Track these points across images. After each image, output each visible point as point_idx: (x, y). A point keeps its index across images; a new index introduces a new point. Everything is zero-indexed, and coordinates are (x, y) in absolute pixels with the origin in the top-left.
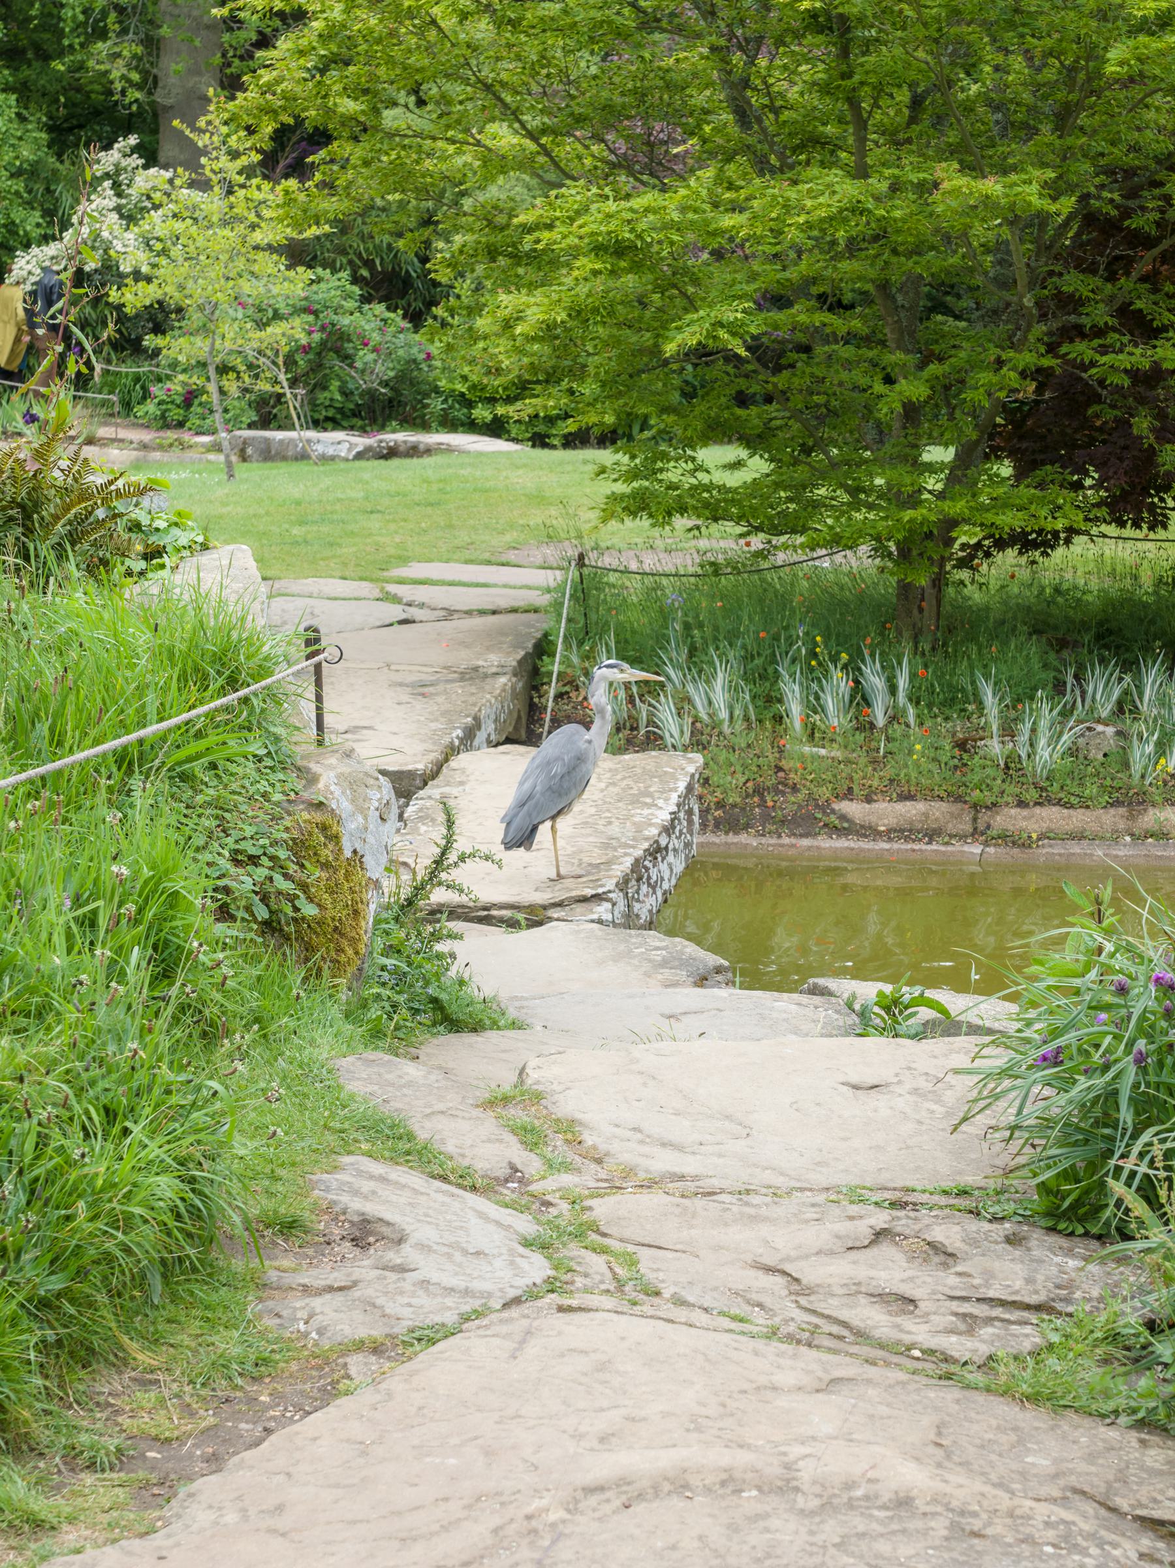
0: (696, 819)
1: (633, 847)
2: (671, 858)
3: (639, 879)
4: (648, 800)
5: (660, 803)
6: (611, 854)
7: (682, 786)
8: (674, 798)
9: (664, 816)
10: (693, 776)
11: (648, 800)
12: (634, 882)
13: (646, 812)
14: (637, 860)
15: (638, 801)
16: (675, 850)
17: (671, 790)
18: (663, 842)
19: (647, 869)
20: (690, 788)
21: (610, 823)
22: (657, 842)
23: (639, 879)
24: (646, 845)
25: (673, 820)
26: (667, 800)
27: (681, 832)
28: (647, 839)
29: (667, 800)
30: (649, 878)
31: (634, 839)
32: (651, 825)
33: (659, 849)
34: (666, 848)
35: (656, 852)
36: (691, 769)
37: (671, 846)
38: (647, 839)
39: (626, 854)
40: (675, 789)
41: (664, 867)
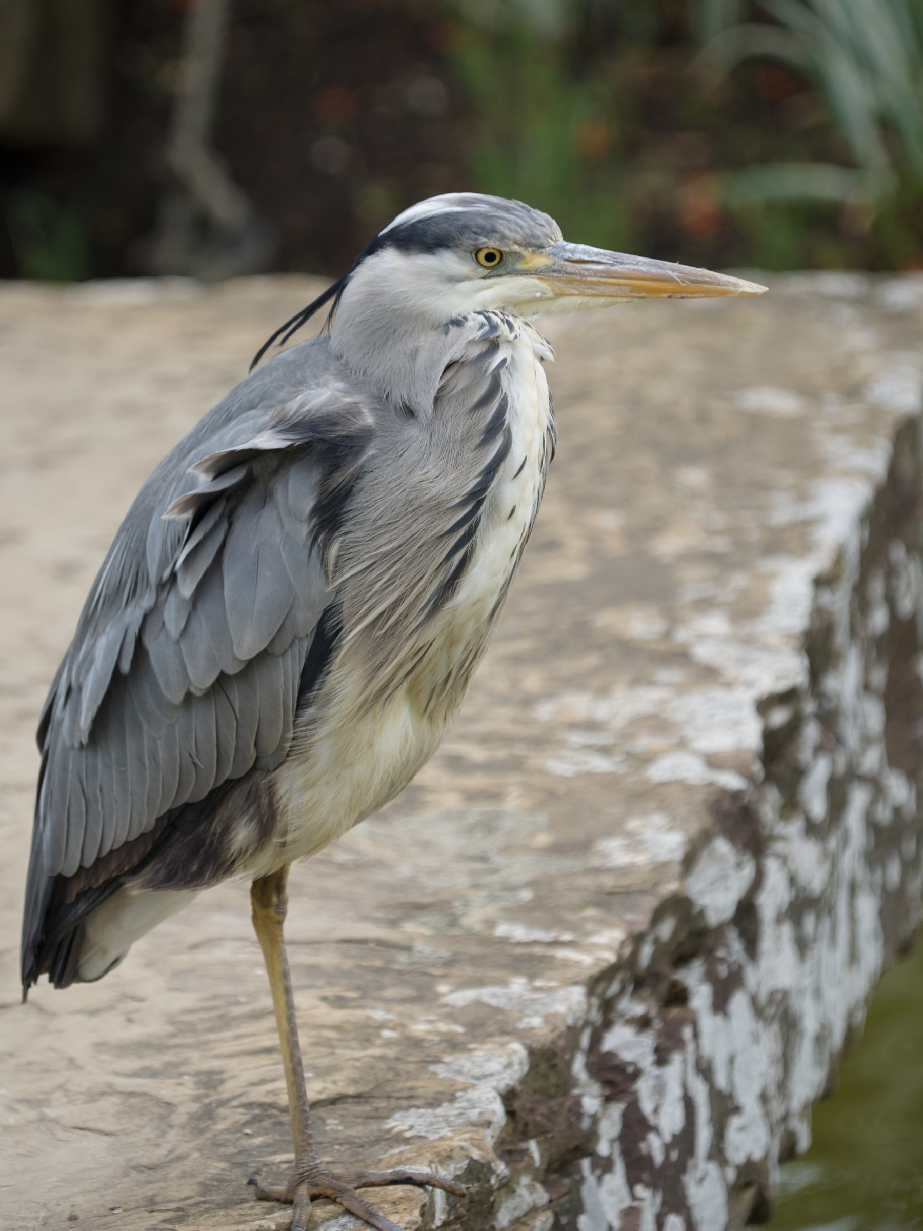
1: (529, 962)
4: (640, 624)
7: (839, 509)
11: (640, 624)
13: (623, 705)
15: (582, 637)
24: (605, 943)
25: (777, 749)
29: (746, 610)
32: (647, 796)
38: (609, 900)
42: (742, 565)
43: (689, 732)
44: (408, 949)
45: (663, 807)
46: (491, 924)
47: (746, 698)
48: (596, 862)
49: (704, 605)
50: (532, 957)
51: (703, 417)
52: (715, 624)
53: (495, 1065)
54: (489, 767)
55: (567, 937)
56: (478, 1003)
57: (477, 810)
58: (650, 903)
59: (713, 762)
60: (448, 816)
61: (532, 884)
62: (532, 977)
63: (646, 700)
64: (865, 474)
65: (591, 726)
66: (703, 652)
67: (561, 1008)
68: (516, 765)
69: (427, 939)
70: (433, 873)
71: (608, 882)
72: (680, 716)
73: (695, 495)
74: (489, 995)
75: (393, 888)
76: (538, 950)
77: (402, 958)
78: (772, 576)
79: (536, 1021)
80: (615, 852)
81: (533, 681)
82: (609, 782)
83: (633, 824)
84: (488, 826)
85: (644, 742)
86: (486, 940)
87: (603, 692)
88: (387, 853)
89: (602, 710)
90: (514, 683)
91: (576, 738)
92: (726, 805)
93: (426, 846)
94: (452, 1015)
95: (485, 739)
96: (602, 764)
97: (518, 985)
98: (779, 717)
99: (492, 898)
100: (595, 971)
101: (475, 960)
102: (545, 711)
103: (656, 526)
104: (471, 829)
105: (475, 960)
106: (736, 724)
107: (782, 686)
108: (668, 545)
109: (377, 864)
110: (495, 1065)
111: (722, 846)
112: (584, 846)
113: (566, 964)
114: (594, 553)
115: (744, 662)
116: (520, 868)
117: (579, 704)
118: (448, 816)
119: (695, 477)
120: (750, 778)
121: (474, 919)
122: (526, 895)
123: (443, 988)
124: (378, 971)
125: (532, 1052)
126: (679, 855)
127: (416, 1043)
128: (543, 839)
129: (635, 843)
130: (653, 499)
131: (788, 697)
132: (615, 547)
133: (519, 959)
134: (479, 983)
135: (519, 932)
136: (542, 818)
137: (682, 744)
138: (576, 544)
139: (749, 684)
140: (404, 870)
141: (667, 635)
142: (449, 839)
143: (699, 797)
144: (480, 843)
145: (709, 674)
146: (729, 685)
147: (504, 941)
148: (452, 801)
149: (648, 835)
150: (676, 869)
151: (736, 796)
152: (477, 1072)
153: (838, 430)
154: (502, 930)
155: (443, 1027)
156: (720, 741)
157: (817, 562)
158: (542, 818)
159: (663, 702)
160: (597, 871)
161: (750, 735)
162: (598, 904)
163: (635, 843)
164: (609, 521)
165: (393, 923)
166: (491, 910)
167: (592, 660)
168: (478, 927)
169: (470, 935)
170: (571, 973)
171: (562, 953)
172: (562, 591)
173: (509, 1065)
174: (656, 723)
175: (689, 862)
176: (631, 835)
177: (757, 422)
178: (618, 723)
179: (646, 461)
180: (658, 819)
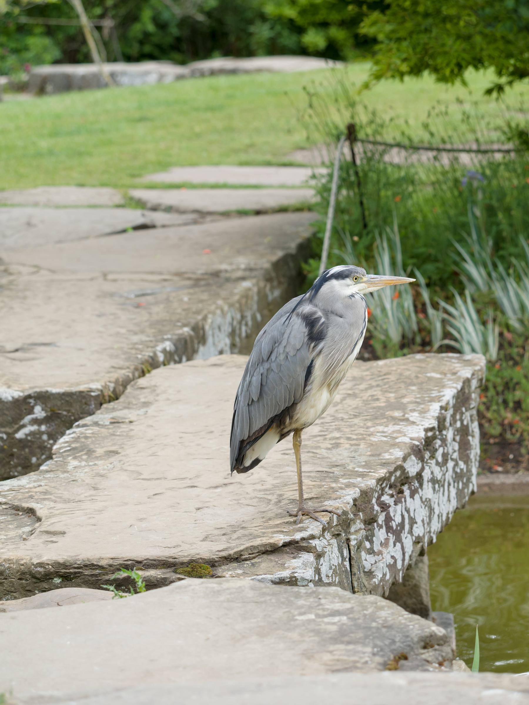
0: (475, 441)
1: (363, 475)
2: (427, 491)
3: (370, 521)
4: (397, 414)
5: (414, 416)
6: (327, 484)
7: (449, 394)
8: (435, 409)
9: (416, 433)
10: (467, 382)
11: (397, 414)
12: (358, 525)
13: (391, 428)
14: (365, 494)
15: (383, 416)
16: (434, 481)
17: (432, 400)
18: (412, 467)
19: (384, 507)
20: (462, 398)
21: (337, 445)
22: (401, 468)
23: (370, 521)
24: (382, 472)
26: (423, 412)
27: (445, 456)
28: (384, 464)
29: (423, 412)
30: (388, 519)
31: (367, 465)
32: (395, 445)
33: (405, 479)
34: (419, 476)
35: (401, 483)
36: (466, 373)
37: (426, 475)
38: (384, 464)
39: (348, 486)
40: (439, 399)
41: (414, 504)
42: (423, 404)
43: (406, 433)
44: (333, 473)
45: (398, 447)
46: (354, 468)
47: (422, 428)
48: (382, 458)
49: (413, 410)
50: (363, 474)
51: (417, 377)
52: (416, 414)
53: (351, 492)
54: (357, 439)
55: (372, 471)
56: (349, 482)
57: (353, 448)
58: (394, 466)
59: (412, 439)
60: (346, 449)
61: (365, 462)
62: (363, 478)
63: (397, 428)
64: (456, 388)
65: (383, 432)
66: (411, 419)
67: (370, 483)
68: (364, 439)
69: (338, 471)
70: (341, 460)
71: (384, 461)
72: (404, 431)
73: (413, 391)
74: (351, 480)
75: (331, 462)
76: (365, 473)
77: (332, 474)
78: (431, 405)
79: (363, 485)
80: (387, 456)
81: (369, 424)
82: (386, 442)
83: (391, 451)
84: (355, 451)
85: (395, 435)
86: (352, 471)
87: (387, 426)
88: (330, 456)
89: (386, 429)
90: (365, 424)
91: (379, 434)
92: (415, 448)
93: (340, 455)
94: (342, 484)
95: (356, 435)
96: (385, 439)
97: (359, 479)
98: (430, 434)
99: (355, 464)
100: (379, 477)
101: (349, 475)
102: (372, 429)
103: (403, 397)
104: (352, 452)
105: (349, 475)
106: (418, 432)
107: (431, 426)
108: (405, 400)
109: (327, 458)
110: (351, 492)
111: (413, 457)
112: (379, 455)
113: (372, 476)
114: (388, 401)
115: (422, 421)
116: (363, 459)
117: (381, 428)
118: (346, 449)
119: (414, 388)
120: (421, 443)
121: (350, 468)
122: (364, 463)
123: (340, 480)
124: (325, 477)
125: (361, 491)
126: (402, 457)
127: (333, 488)
128: (369, 453)
129: (391, 454)
130: (404, 392)
131: (432, 429)
132: (393, 400)
133: (361, 475)
134: (350, 479)
135: (361, 470)
136: (369, 449)
137: (405, 435)
138: (383, 399)
139: (422, 425)
140: (334, 459)
141: (404, 416)
142: (346, 454)
143: (408, 445)
144: (353, 454)
145: (413, 423)
146: (418, 425)
147: (357, 471)
148: (347, 446)
149: (395, 452)
150: (401, 459)
151: (418, 446)
152: (347, 494)
153: (449, 380)
154: (356, 469)
155: (339, 485)
156: (415, 435)
157: (443, 404)
158: (369, 449)
159: (401, 428)
160: (382, 459)
161: (422, 434)
162: (381, 465)
163: (391, 454)
164: (392, 395)
165: (330, 468)
166: (354, 466)
167: (385, 420)
168: (351, 469)
169: (348, 470)
170: (373, 477)
171: (370, 474)
172: (379, 408)
173: (355, 493)
174: (399, 432)
175: (405, 459)
176: (390, 453)
177: (430, 379)
178: (389, 432)
179: (403, 385)
180: (397, 449)
